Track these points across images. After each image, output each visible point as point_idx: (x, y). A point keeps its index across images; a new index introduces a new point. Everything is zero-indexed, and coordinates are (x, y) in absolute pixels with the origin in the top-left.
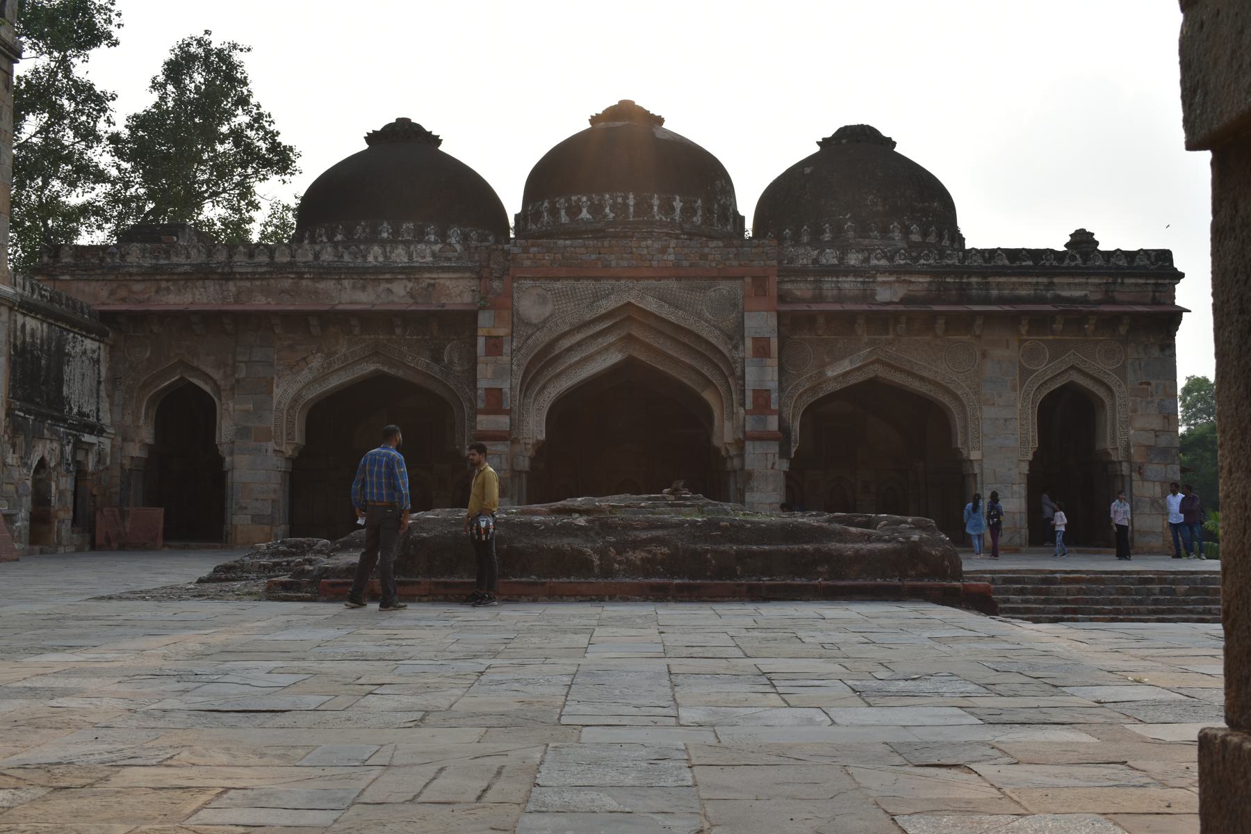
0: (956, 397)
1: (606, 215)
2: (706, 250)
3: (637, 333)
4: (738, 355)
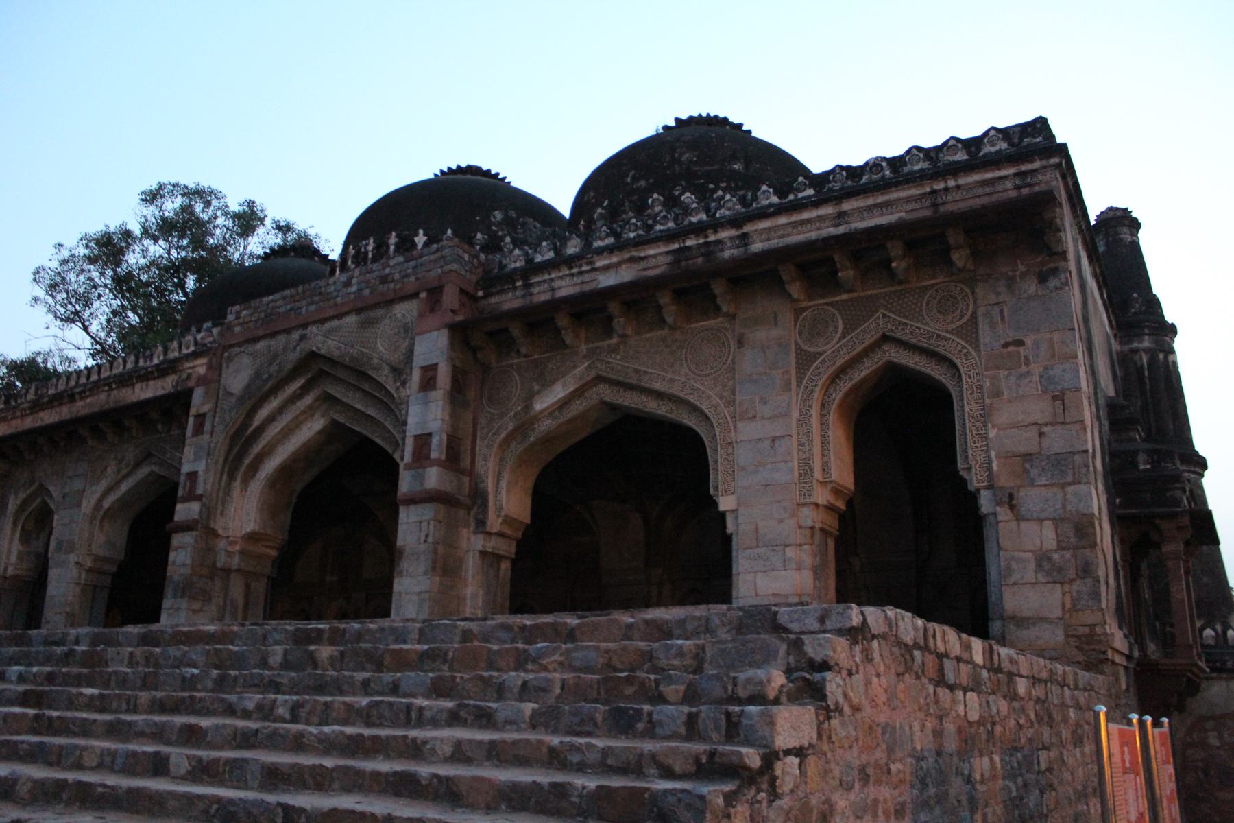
2: (387, 271)
3: (336, 391)
4: (404, 393)
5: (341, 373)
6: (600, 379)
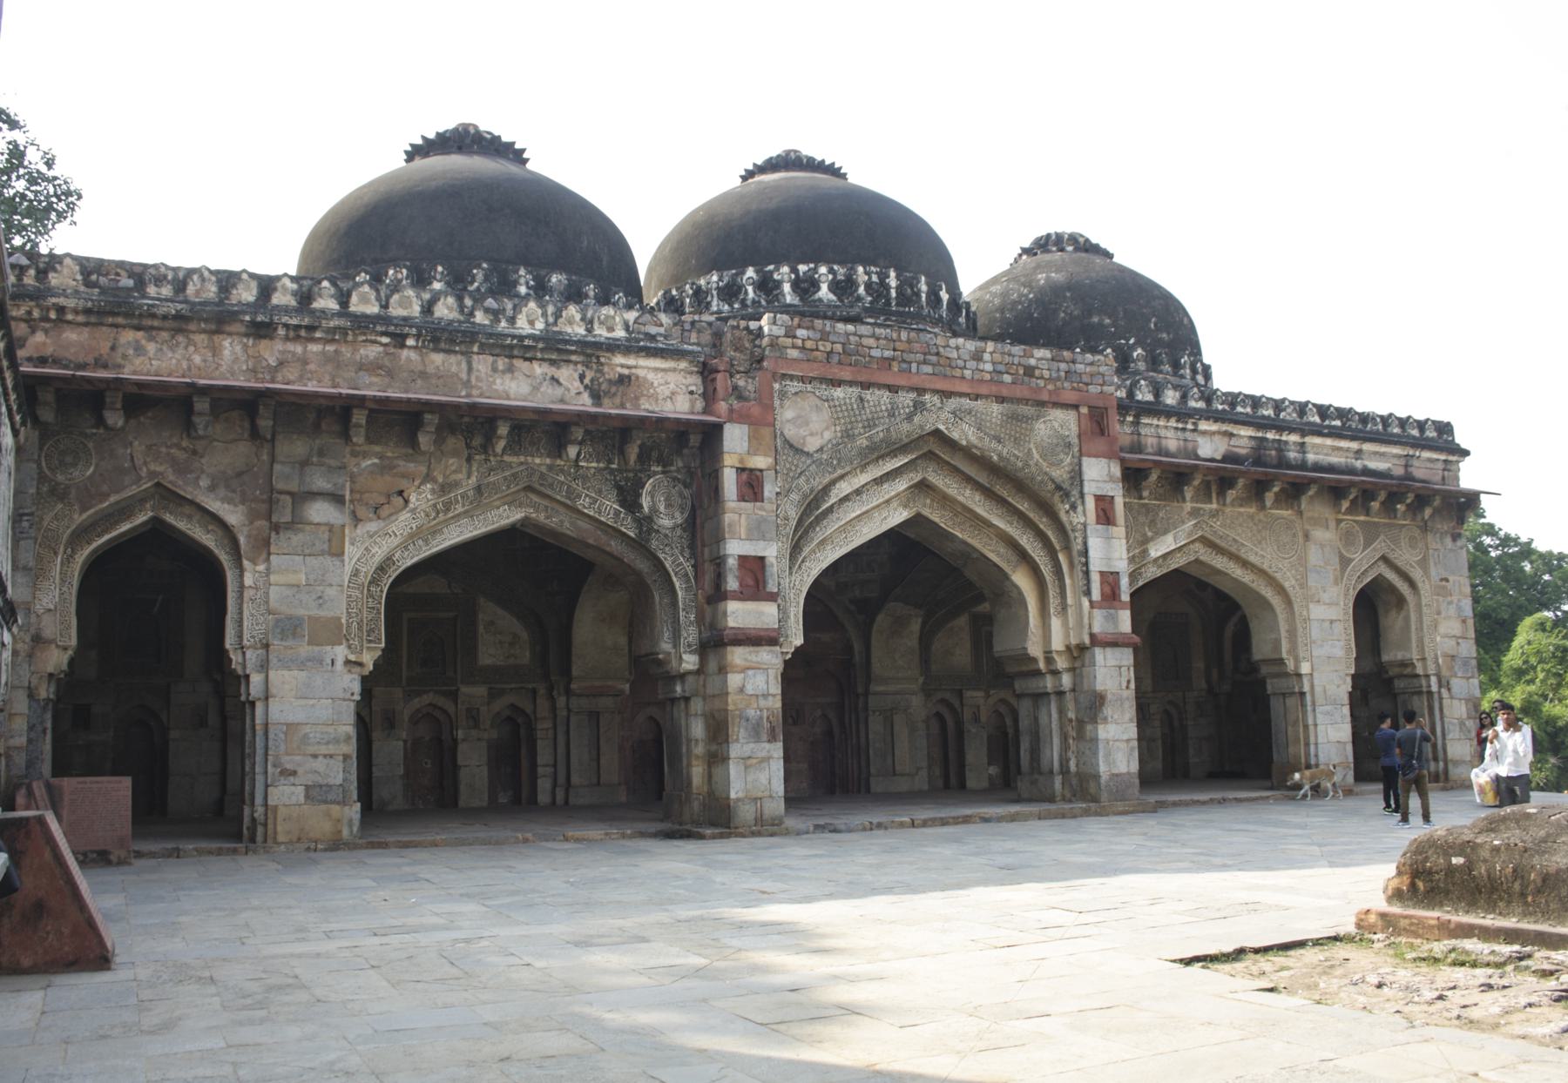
0: (1281, 590)
1: (859, 299)
4: (1077, 519)
5: (958, 462)
6: (1204, 540)
